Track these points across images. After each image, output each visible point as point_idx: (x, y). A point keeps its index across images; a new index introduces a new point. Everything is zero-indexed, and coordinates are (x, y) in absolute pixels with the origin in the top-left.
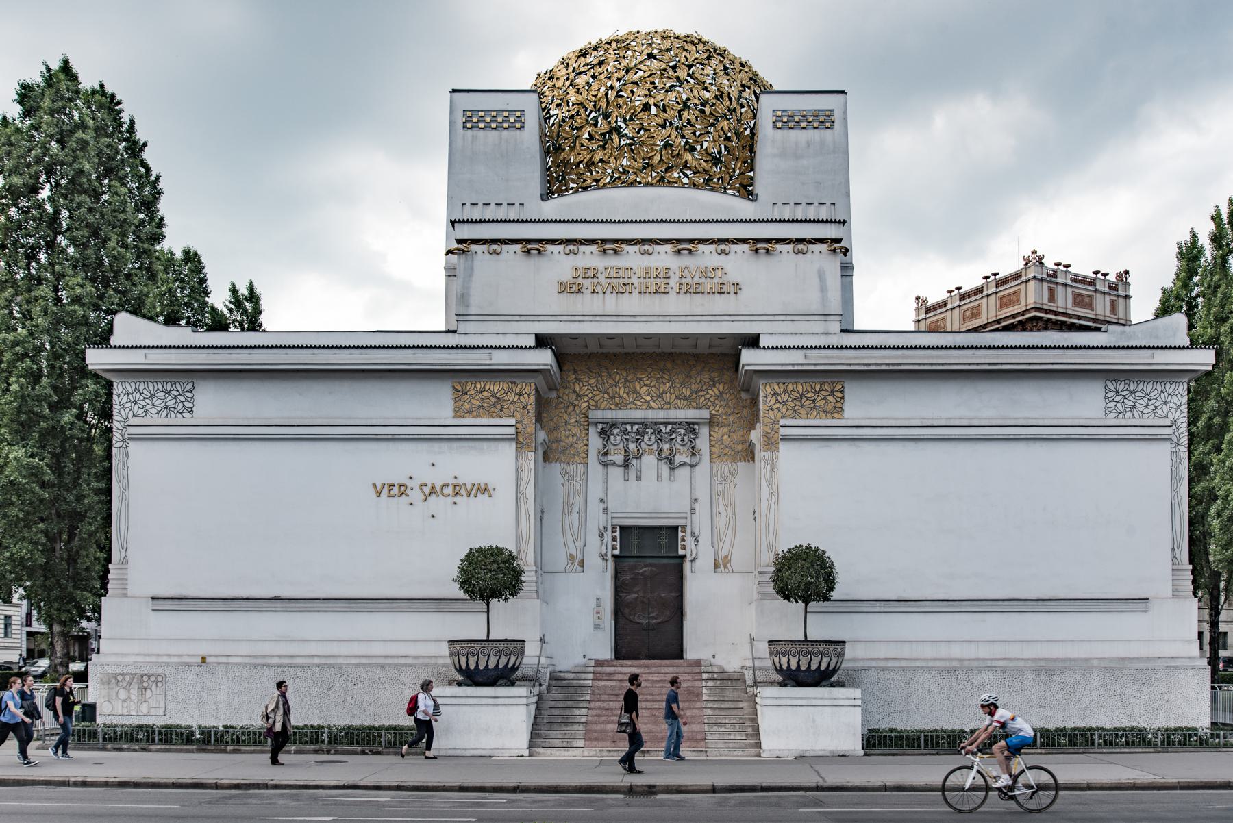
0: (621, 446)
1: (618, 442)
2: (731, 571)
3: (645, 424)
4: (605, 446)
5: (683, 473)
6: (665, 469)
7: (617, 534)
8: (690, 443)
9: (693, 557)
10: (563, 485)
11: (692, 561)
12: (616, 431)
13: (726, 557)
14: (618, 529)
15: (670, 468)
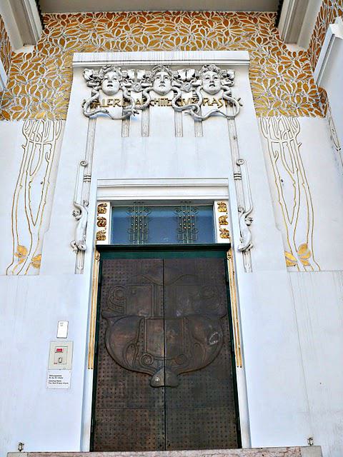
0: (119, 96)
1: (114, 89)
2: (316, 268)
3: (156, 68)
4: (93, 94)
5: (216, 127)
6: (187, 121)
7: (107, 215)
8: (223, 91)
9: (246, 244)
10: (24, 147)
11: (243, 251)
12: (111, 75)
13: (305, 247)
14: (108, 208)
15: (195, 121)
